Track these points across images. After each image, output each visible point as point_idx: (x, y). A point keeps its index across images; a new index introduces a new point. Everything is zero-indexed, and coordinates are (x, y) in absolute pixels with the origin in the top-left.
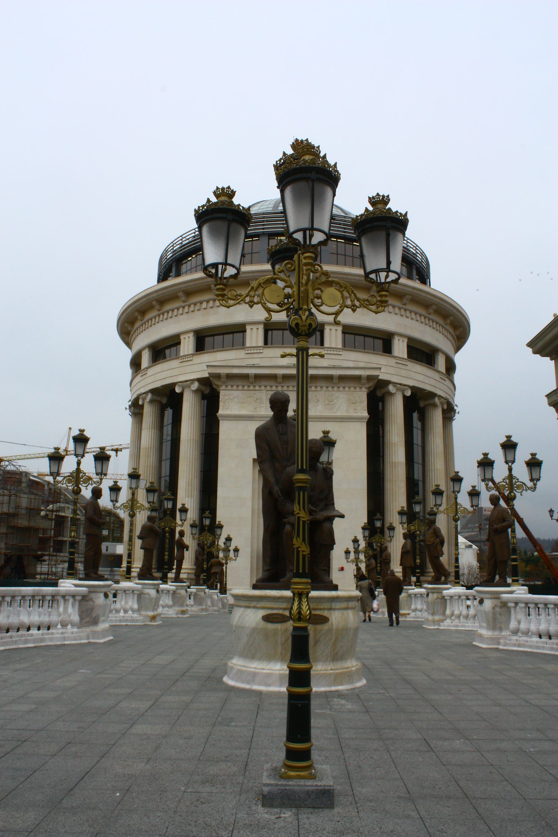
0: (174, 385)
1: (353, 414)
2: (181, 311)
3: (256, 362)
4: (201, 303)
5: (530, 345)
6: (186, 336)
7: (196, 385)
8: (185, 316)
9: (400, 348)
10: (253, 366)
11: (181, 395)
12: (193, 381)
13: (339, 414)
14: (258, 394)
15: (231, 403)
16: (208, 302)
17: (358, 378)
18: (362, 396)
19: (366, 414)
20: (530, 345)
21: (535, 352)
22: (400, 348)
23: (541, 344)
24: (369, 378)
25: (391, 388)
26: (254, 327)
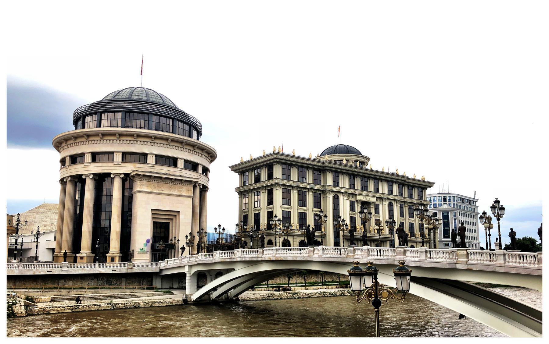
0: (110, 174)
2: (115, 141)
3: (152, 170)
4: (127, 140)
5: (230, 167)
7: (122, 176)
8: (117, 144)
9: (200, 169)
12: (121, 174)
13: (183, 194)
14: (154, 184)
15: (139, 186)
16: (130, 141)
17: (191, 181)
22: (200, 169)
23: (236, 168)
26: (151, 156)
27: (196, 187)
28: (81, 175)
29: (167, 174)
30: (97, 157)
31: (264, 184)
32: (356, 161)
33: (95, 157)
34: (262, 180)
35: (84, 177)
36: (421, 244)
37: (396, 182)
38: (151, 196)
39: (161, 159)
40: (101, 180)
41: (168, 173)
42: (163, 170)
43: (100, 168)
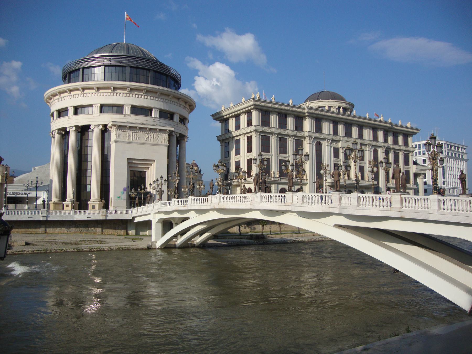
0: (90, 125)
1: (163, 143)
5: (212, 116)
6: (96, 106)
7: (101, 127)
9: (176, 118)
10: (127, 123)
11: (93, 130)
12: (99, 125)
18: (166, 137)
19: (168, 144)
20: (212, 116)
21: (213, 119)
23: (217, 117)
24: (170, 131)
25: (173, 133)
27: (172, 135)
28: (66, 128)
29: (143, 124)
30: (79, 110)
31: (244, 132)
32: (339, 108)
33: (77, 110)
34: (241, 127)
35: (68, 130)
36: (40, 185)
37: (381, 129)
38: (127, 145)
39: (136, 110)
40: (83, 130)
41: (145, 122)
42: (138, 120)
43: (81, 120)
